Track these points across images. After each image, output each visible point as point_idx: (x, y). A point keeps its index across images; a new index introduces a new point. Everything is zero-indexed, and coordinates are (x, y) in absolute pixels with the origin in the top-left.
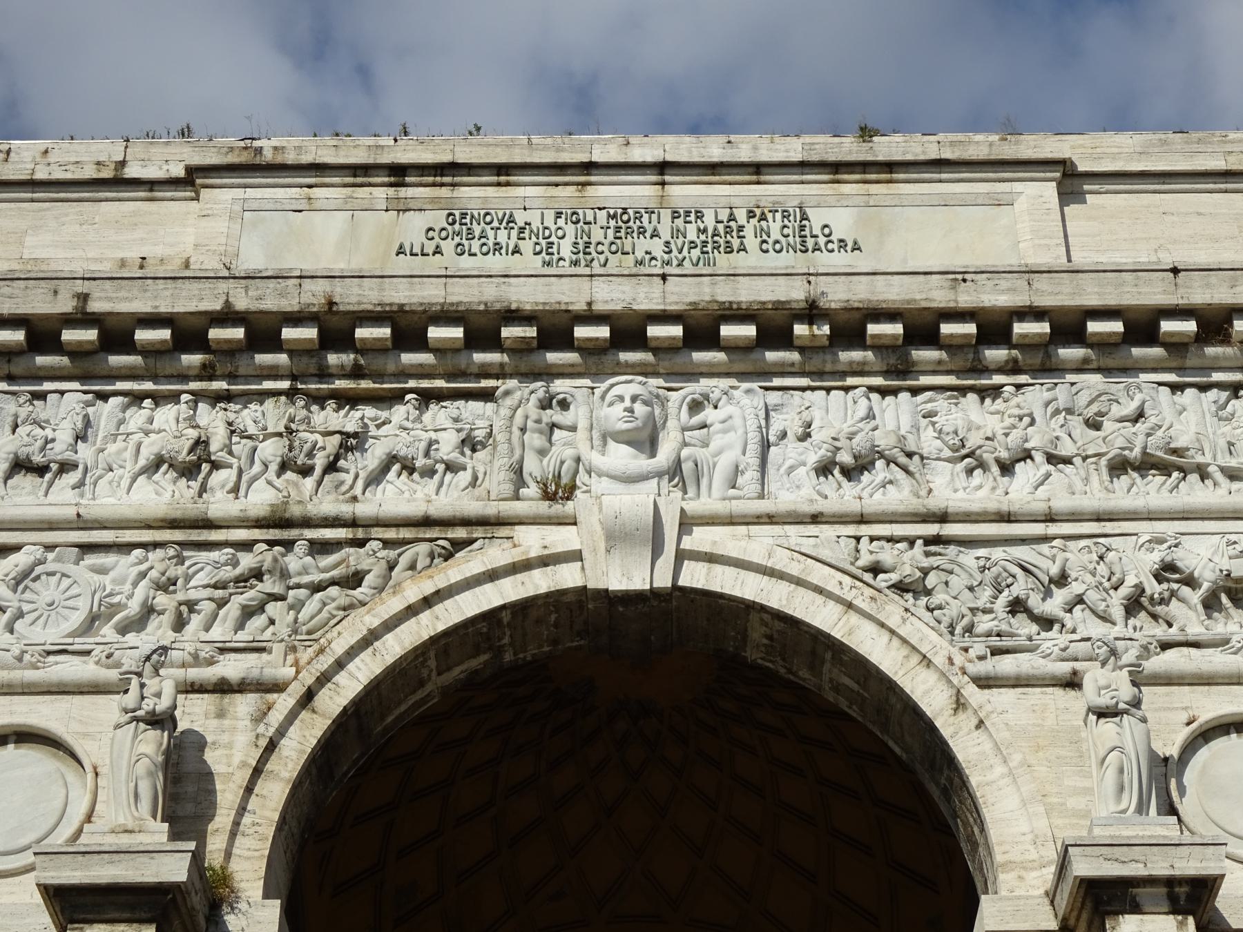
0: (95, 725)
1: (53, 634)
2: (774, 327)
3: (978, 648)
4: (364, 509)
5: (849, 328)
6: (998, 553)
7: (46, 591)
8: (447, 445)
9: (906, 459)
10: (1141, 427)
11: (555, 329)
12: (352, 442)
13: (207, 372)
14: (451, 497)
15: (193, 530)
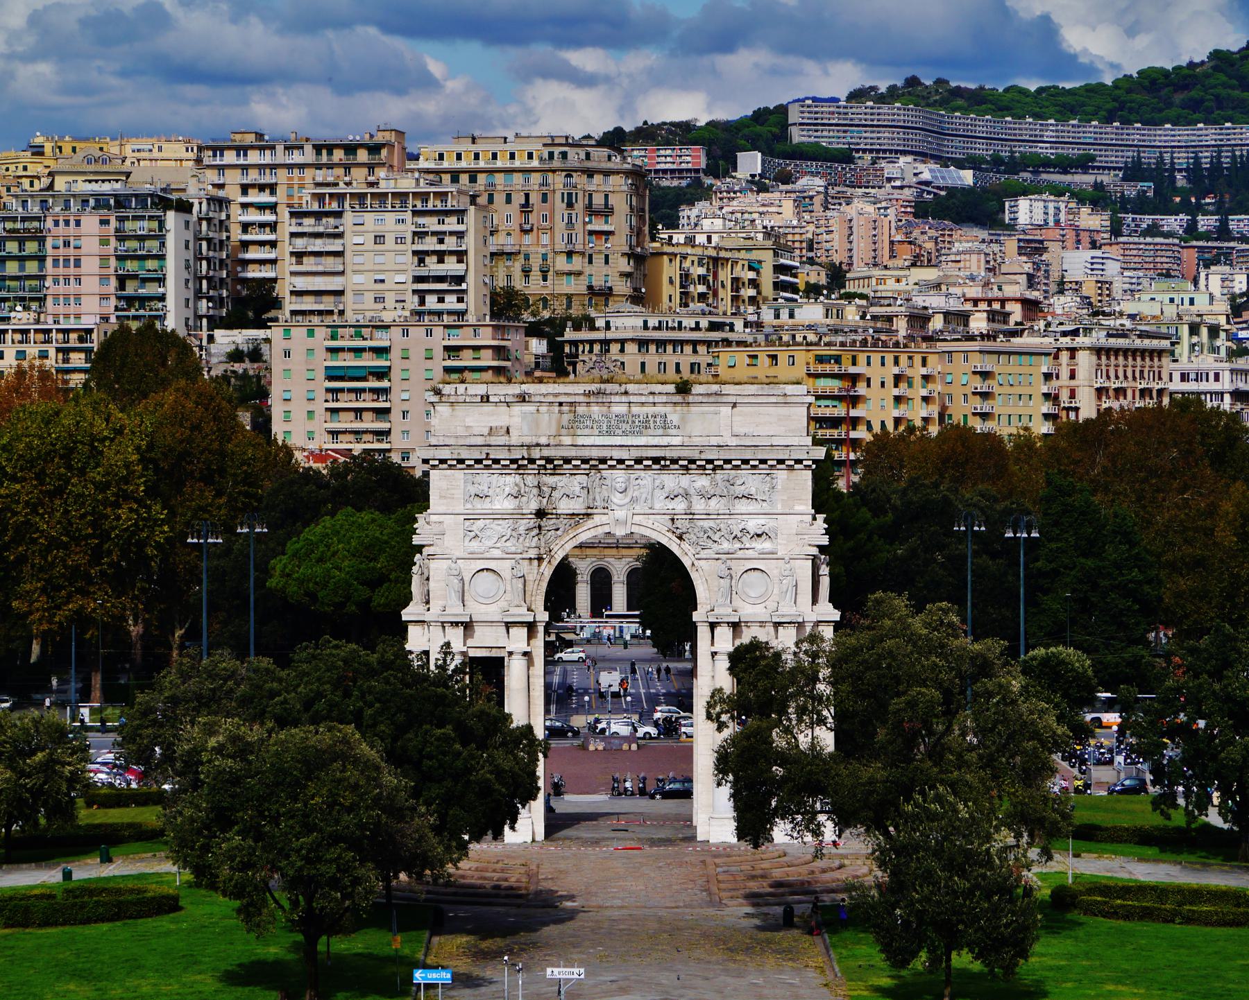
0: (504, 567)
1: (490, 543)
2: (656, 460)
3: (699, 548)
4: (559, 512)
5: (674, 461)
6: (706, 524)
7: (488, 533)
8: (577, 489)
9: (686, 495)
10: (743, 487)
11: (603, 461)
12: (554, 489)
13: (518, 468)
14: (577, 506)
15: (518, 515)
